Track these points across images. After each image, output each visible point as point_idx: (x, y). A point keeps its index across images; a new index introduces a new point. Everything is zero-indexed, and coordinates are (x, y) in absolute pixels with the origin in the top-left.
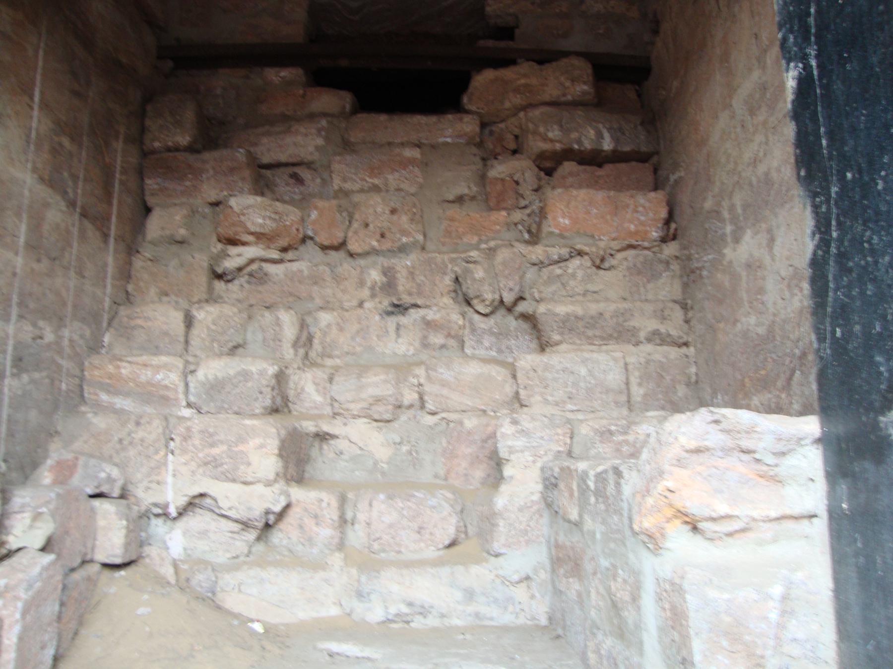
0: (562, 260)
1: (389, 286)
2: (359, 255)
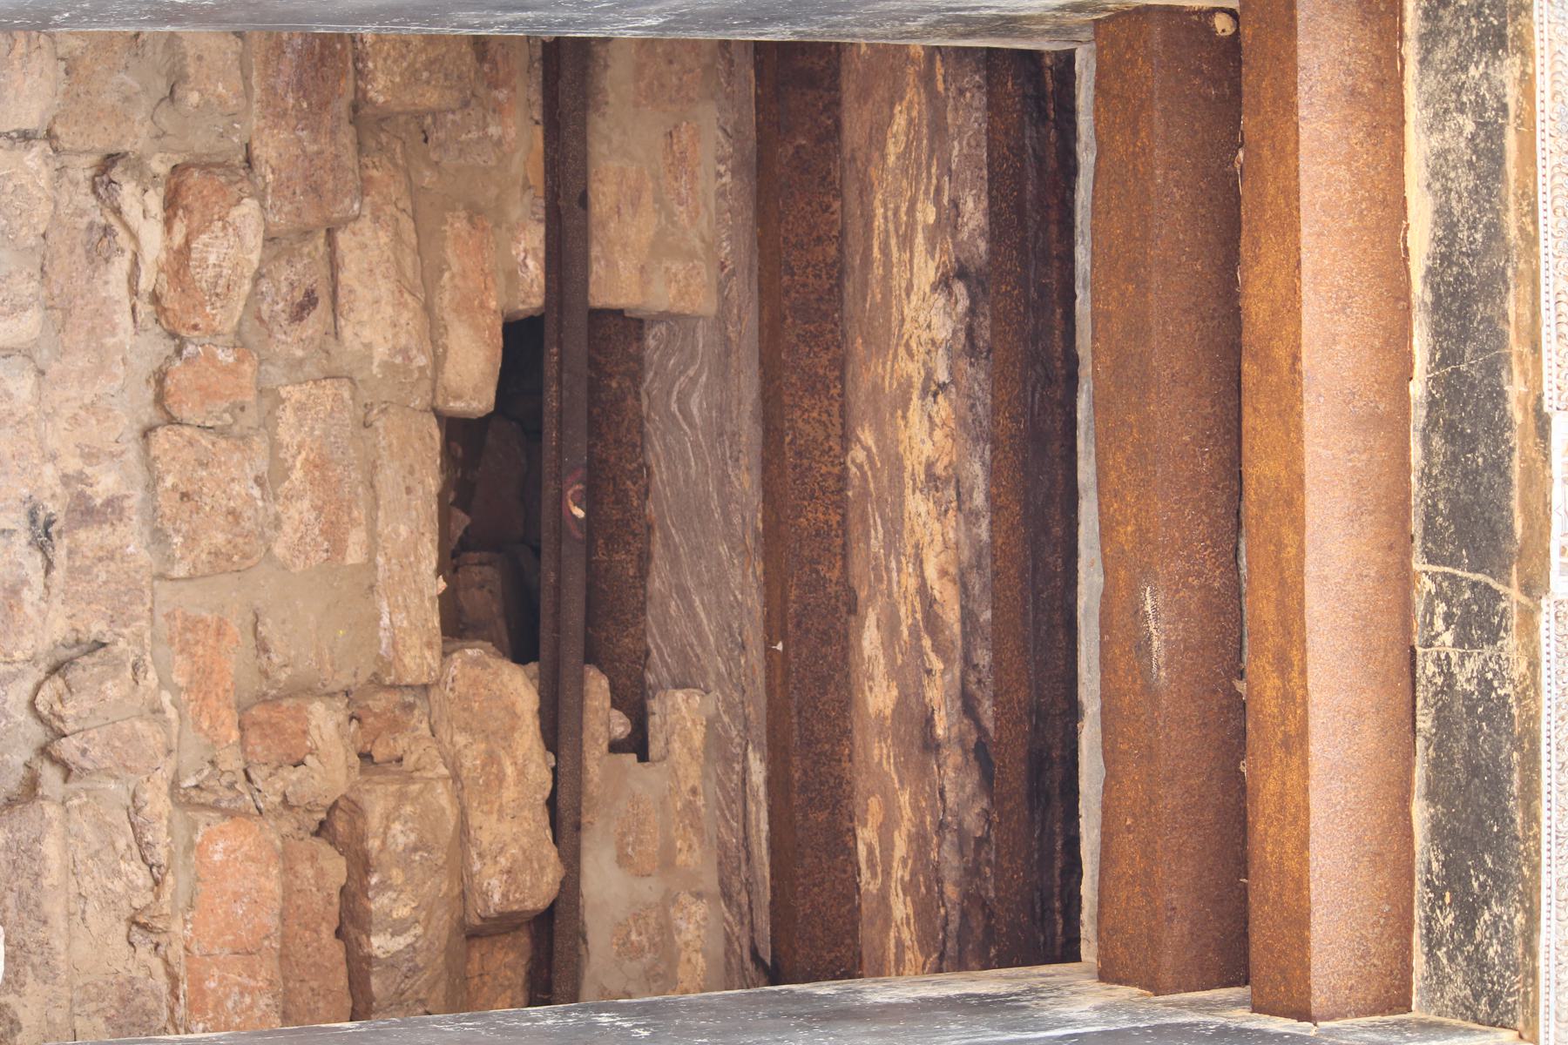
0: (143, 848)
1: (86, 512)
2: (146, 450)
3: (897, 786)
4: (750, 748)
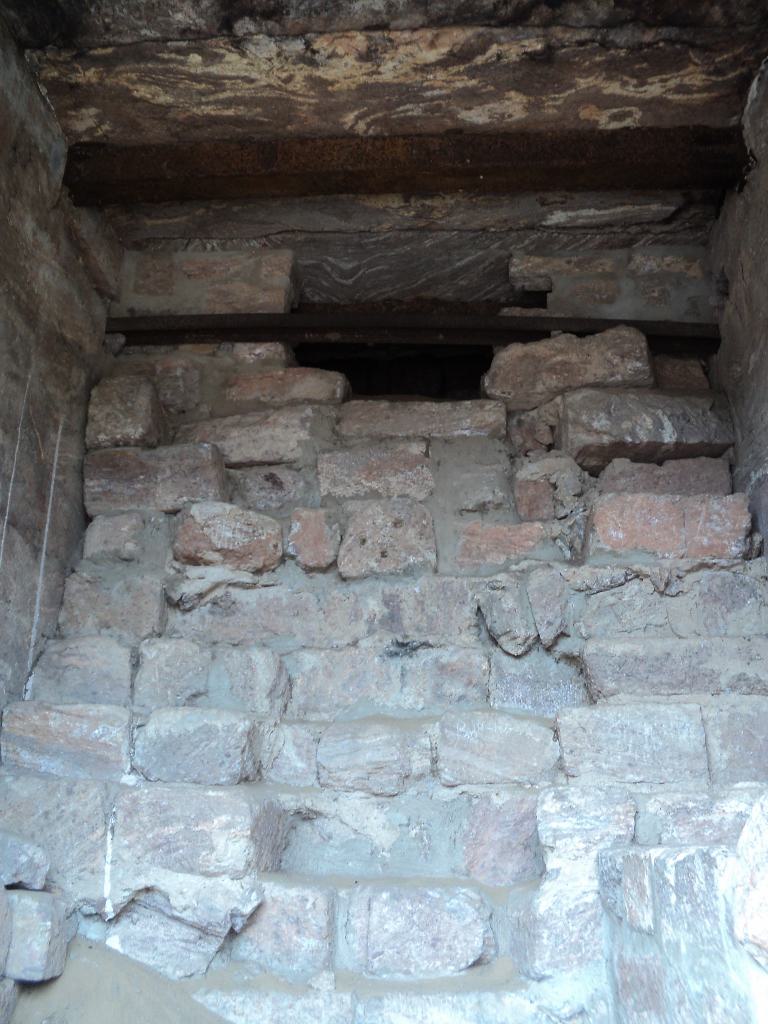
0: (615, 585)
1: (392, 619)
2: (354, 579)
3: (573, 91)
4: (544, 223)
